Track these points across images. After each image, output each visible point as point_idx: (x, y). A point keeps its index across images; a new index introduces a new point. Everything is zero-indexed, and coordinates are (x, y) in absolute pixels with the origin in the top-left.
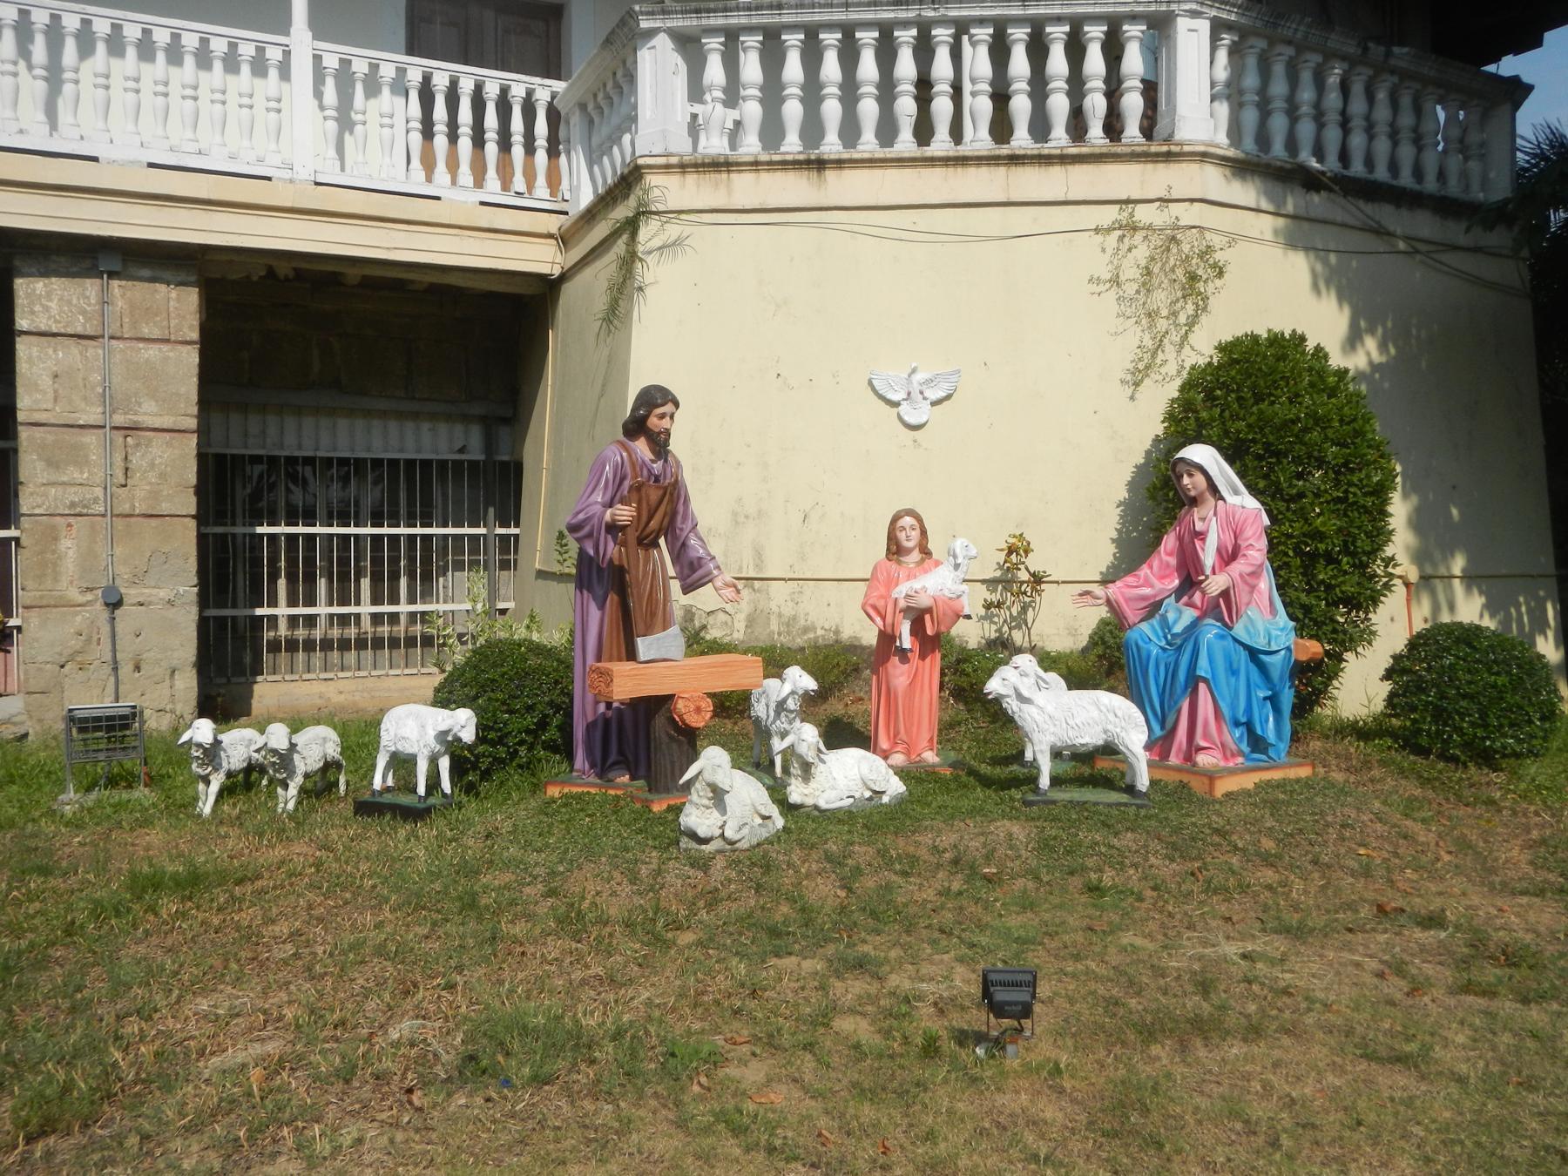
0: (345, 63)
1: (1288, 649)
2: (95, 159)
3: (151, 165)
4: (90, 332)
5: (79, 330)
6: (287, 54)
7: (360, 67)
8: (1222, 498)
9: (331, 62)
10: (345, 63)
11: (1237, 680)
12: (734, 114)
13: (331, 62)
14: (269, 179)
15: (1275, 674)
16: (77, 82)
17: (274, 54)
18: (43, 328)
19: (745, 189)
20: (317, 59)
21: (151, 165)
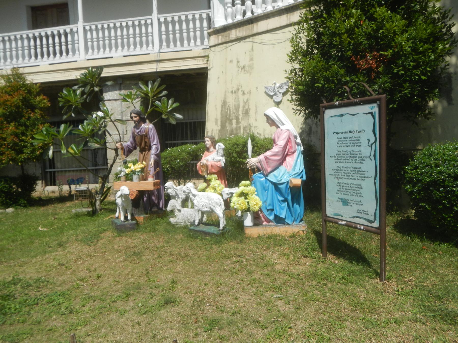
0: (166, 19)
1: (288, 182)
2: (112, 57)
3: (124, 56)
4: (118, 98)
5: (115, 98)
6: (152, 20)
7: (169, 19)
8: (279, 127)
9: (162, 20)
10: (166, 19)
11: (268, 192)
12: (244, 8)
13: (162, 20)
14: (149, 54)
15: (284, 191)
16: (78, 43)
17: (149, 21)
18: (108, 99)
19: (234, 34)
20: (159, 20)
21: (124, 56)
